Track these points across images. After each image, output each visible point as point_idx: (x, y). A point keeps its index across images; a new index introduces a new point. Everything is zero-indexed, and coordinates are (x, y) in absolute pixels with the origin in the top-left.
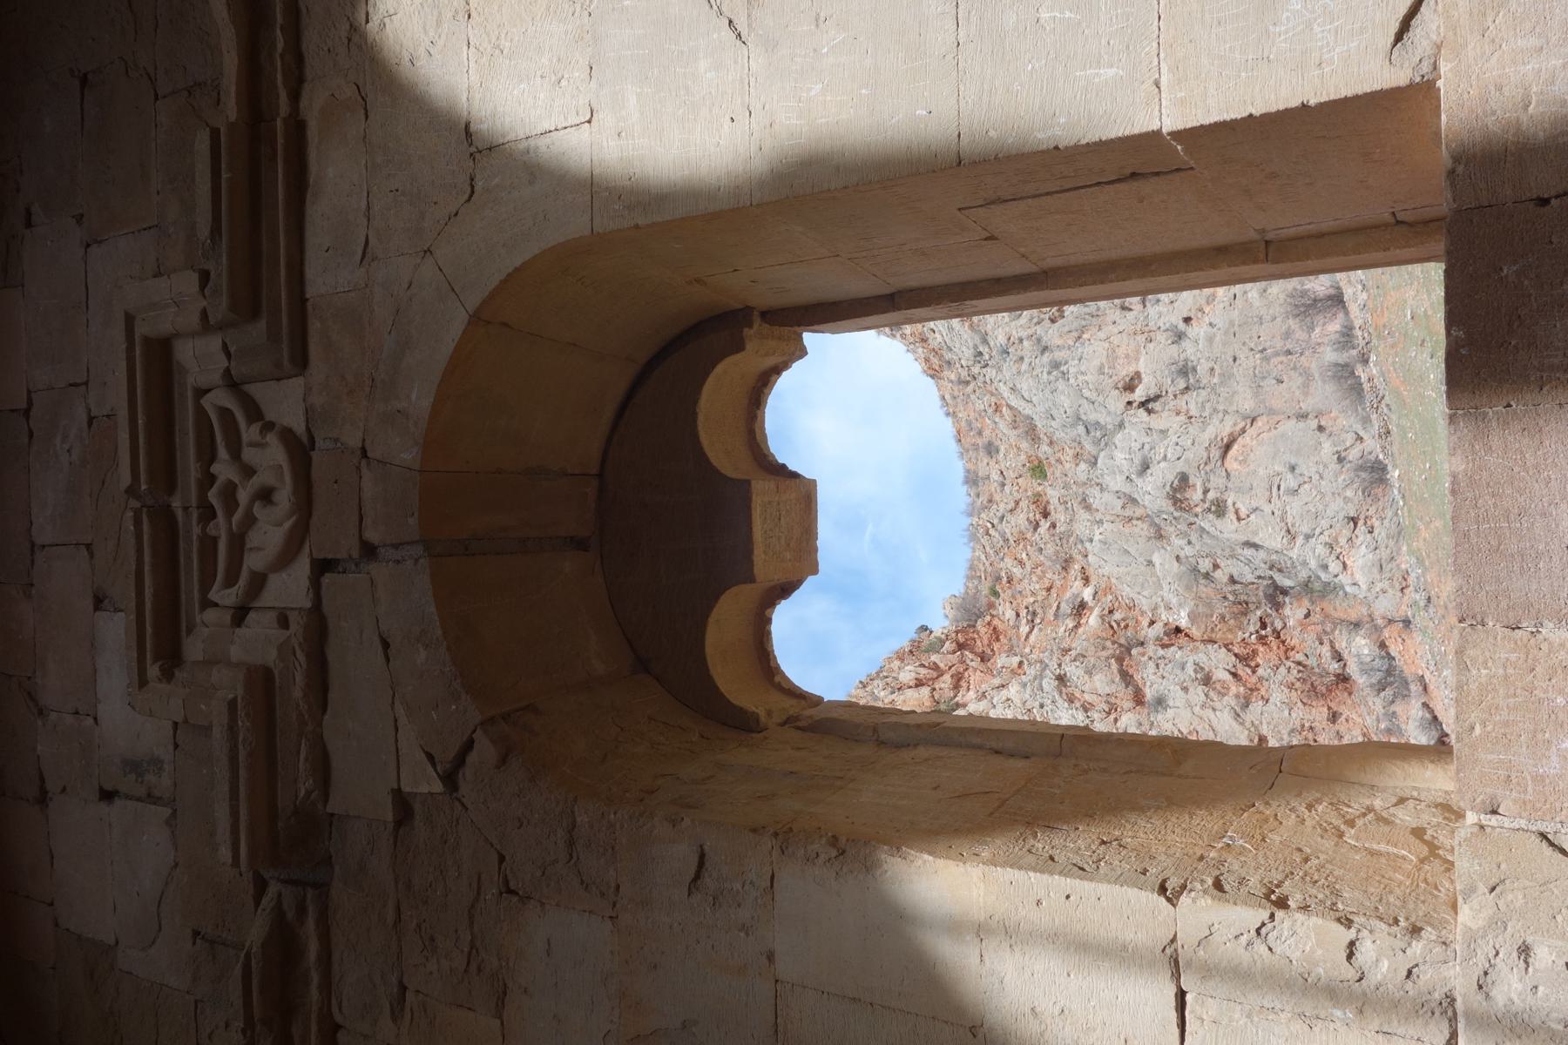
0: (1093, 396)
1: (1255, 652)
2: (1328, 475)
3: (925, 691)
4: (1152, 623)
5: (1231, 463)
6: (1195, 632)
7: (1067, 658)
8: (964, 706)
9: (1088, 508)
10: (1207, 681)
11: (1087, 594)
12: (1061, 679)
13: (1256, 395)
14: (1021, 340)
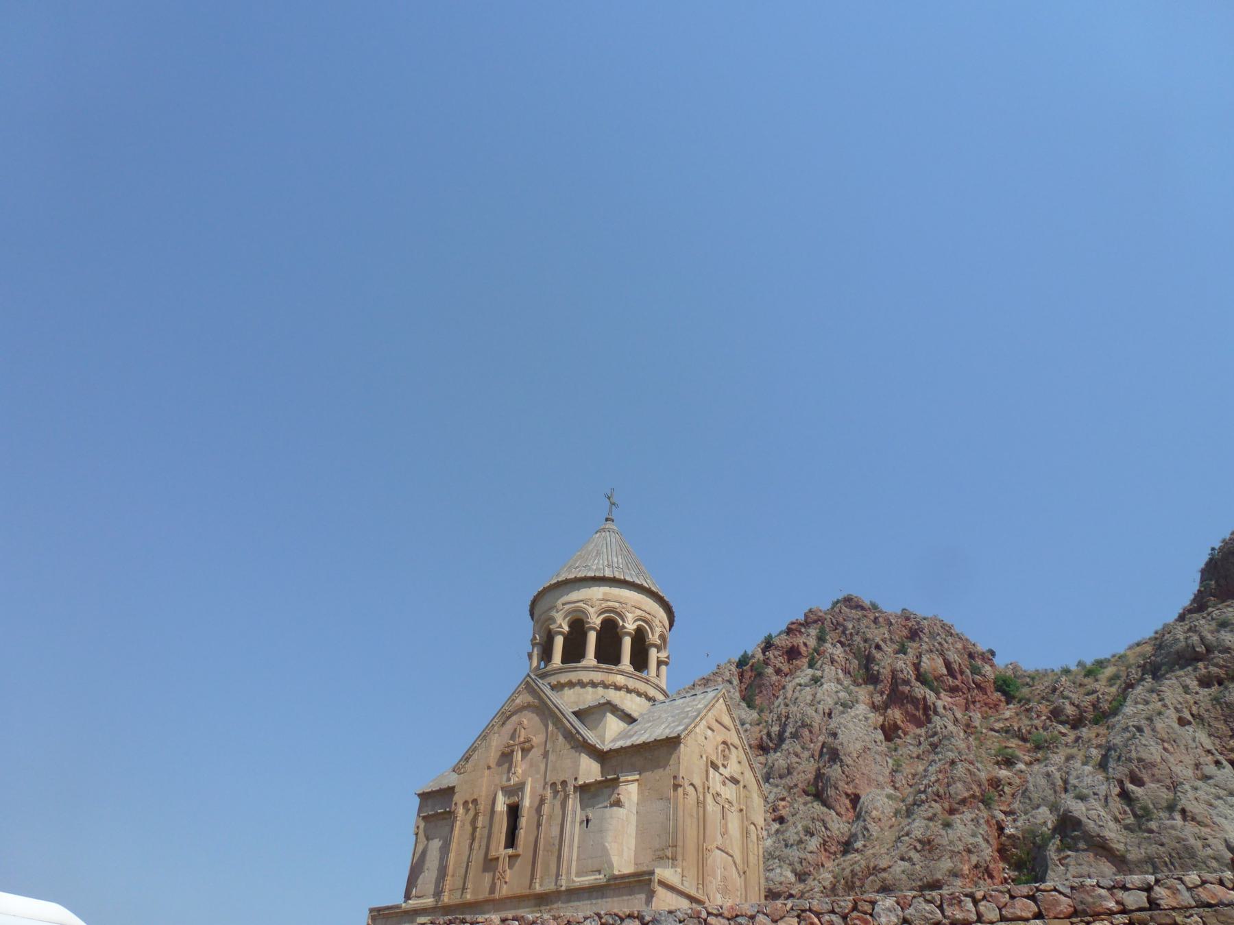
3: (945, 671)
4: (1004, 812)
7: (966, 765)
11: (1021, 766)
12: (953, 763)
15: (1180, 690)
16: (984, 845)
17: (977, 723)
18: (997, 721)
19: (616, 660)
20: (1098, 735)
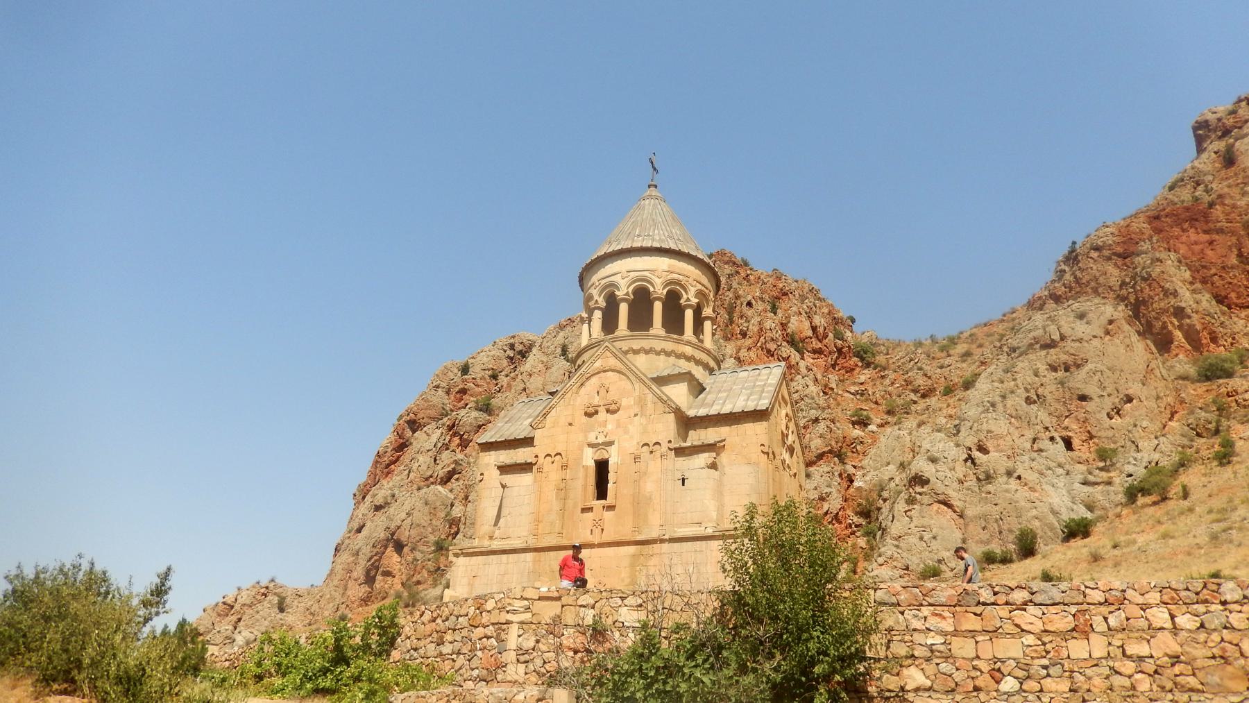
0: (975, 429)
1: (840, 523)
2: (931, 555)
3: (810, 333)
4: (855, 467)
5: (936, 506)
6: (851, 490)
8: (803, 358)
9: (919, 425)
10: (822, 499)
11: (872, 427)
12: (816, 420)
13: (975, 517)
14: (1015, 380)
15: (1031, 373)
16: (835, 494)
17: (833, 385)
18: (854, 384)
19: (680, 330)
20: (948, 406)
